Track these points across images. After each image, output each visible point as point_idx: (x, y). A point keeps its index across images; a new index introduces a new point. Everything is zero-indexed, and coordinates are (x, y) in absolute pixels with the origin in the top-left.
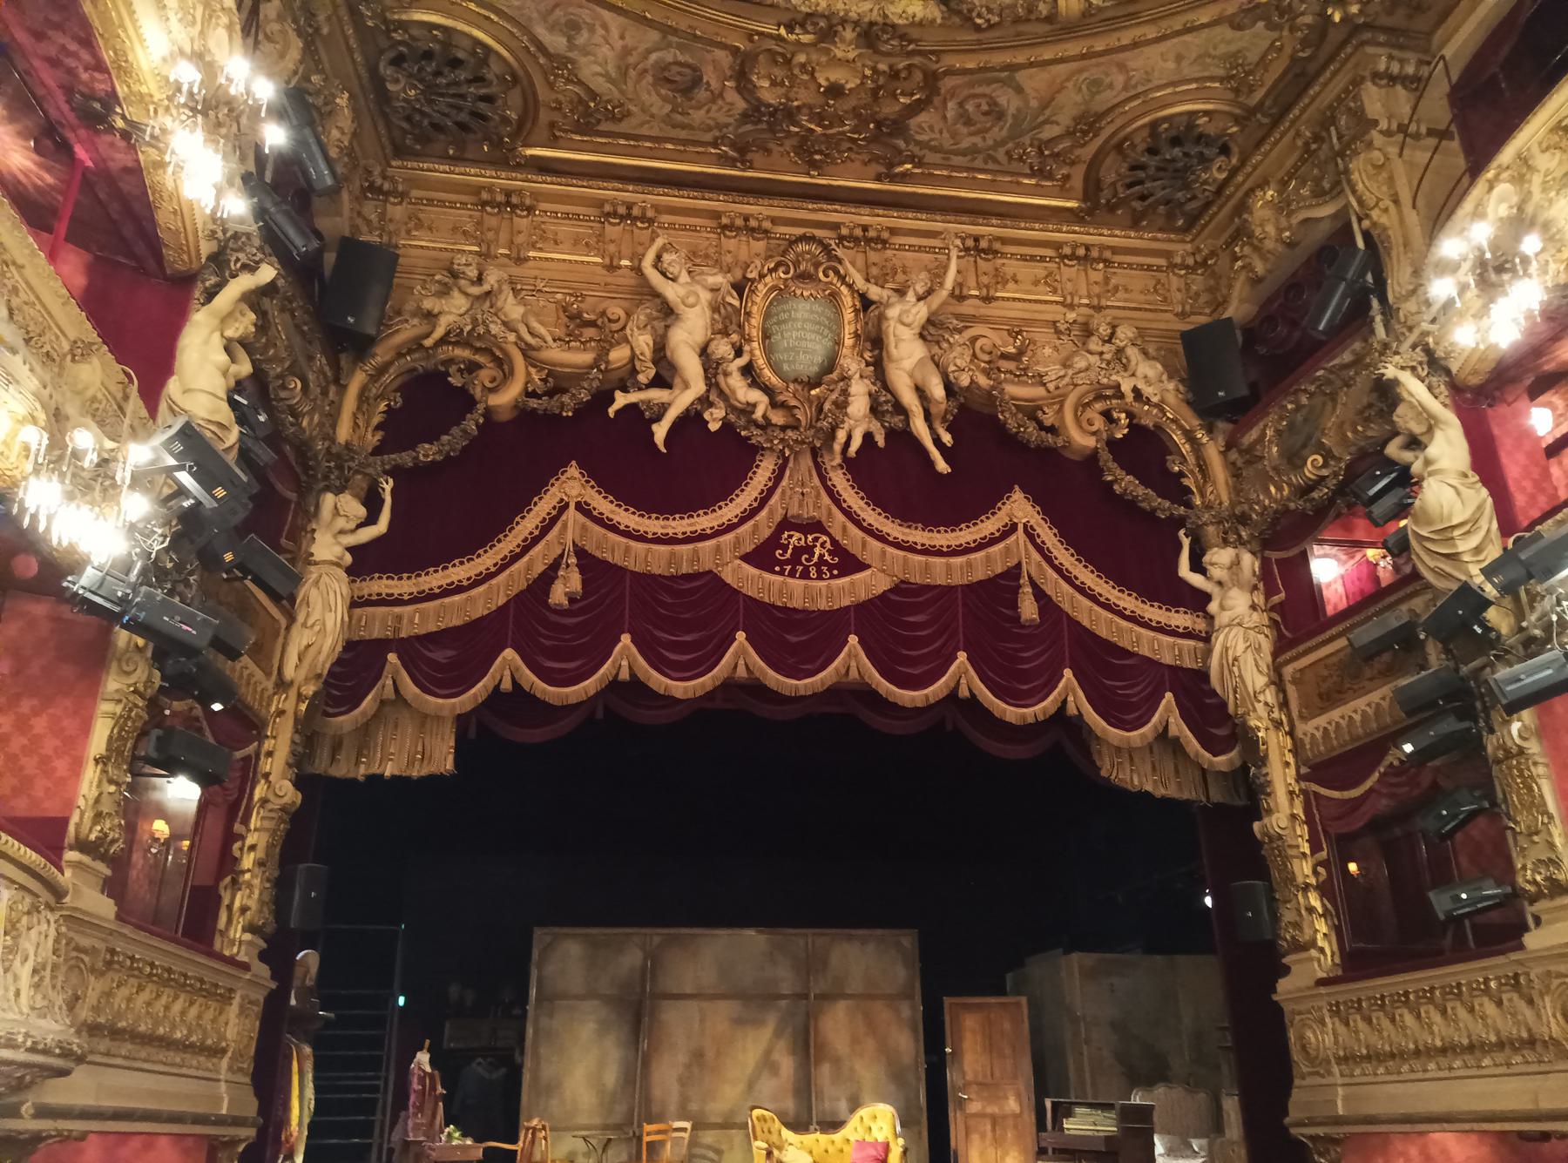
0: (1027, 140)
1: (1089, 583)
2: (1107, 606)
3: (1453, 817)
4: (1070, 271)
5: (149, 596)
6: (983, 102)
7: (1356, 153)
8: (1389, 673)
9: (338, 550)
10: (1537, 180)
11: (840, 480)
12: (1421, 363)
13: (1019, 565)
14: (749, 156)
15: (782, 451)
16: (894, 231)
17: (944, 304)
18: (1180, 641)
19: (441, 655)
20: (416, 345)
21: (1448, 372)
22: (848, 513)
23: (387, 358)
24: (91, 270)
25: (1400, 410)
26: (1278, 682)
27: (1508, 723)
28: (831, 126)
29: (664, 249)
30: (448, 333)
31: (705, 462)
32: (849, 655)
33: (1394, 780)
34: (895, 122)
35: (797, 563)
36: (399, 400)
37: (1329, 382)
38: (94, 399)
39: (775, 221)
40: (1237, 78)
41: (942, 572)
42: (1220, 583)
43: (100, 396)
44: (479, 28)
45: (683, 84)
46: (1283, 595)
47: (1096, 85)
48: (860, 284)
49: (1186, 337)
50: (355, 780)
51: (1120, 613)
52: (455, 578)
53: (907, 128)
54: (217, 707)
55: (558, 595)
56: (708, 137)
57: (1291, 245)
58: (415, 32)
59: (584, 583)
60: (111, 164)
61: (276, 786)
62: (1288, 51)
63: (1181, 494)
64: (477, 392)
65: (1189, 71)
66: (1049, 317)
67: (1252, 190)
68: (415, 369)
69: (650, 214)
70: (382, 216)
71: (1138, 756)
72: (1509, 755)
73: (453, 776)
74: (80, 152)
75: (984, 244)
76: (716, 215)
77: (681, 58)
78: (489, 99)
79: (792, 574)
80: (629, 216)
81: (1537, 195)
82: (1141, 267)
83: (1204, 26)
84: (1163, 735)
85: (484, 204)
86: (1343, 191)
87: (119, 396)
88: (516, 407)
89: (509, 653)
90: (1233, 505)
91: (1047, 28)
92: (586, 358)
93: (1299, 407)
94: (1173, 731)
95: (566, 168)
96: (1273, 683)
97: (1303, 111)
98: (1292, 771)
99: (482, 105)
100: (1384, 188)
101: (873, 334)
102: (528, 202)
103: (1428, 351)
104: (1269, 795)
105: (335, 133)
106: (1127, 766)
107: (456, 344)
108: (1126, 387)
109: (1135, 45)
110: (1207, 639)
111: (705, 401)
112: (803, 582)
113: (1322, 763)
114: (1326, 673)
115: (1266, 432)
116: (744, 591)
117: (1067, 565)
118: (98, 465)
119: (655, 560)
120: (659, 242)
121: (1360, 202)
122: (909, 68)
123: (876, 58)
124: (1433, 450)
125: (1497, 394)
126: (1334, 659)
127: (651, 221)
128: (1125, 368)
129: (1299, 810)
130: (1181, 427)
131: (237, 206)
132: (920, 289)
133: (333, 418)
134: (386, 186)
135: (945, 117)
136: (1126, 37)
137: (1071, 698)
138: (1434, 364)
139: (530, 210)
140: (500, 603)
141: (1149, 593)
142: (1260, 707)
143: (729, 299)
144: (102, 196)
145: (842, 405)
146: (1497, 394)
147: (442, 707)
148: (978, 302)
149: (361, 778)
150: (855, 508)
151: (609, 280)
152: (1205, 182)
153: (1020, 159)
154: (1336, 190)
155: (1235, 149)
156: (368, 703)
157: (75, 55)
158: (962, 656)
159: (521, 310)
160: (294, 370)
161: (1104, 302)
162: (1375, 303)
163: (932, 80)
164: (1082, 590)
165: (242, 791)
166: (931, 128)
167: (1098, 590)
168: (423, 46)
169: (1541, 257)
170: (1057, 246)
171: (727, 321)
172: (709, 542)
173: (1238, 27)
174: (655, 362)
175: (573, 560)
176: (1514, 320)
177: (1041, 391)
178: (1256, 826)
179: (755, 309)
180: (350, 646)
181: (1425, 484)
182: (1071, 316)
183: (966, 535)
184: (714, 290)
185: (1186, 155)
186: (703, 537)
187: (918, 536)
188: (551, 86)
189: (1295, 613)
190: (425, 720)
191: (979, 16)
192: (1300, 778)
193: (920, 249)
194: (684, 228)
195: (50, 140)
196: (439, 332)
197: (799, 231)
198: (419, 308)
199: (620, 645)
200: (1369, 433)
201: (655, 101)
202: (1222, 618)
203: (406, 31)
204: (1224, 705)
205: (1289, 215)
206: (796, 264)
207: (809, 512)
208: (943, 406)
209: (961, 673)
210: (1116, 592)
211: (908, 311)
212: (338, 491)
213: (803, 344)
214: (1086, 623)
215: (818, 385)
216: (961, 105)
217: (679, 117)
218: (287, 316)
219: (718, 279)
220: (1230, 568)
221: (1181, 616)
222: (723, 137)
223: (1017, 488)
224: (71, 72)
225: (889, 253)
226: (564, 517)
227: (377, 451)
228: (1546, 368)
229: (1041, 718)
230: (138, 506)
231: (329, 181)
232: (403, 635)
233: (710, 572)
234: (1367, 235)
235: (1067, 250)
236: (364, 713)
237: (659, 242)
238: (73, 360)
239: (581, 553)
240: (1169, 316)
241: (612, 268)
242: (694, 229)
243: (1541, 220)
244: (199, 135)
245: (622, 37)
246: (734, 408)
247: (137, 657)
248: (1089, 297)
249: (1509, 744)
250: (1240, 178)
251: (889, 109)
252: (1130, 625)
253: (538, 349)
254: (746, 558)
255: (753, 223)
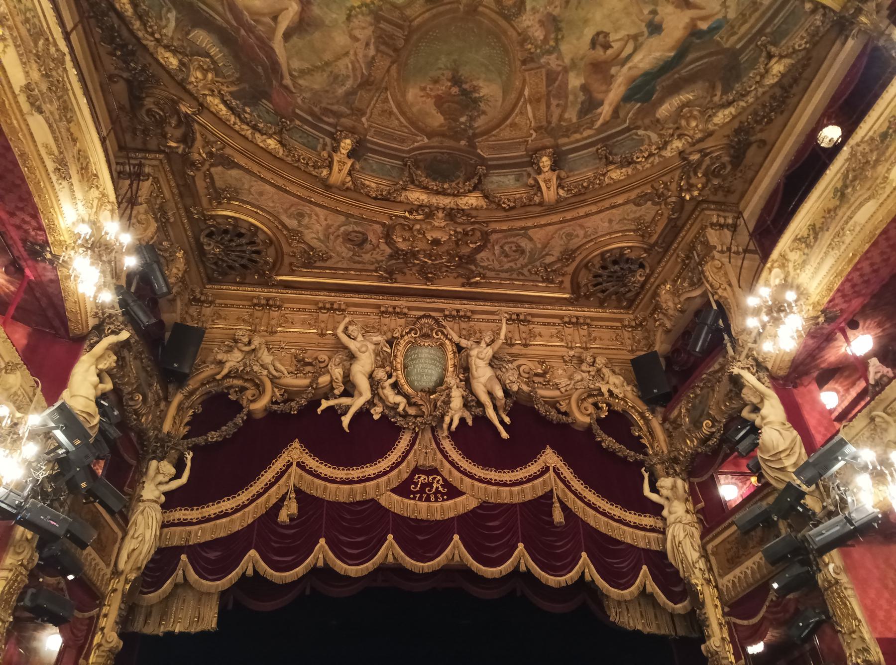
0: (538, 263)
1: (593, 500)
2: (604, 514)
3: (806, 626)
4: (569, 330)
5: (33, 504)
6: (513, 245)
7: (706, 262)
8: (762, 541)
9: (157, 493)
10: (791, 265)
11: (447, 445)
12: (752, 366)
13: (552, 490)
14: (394, 276)
15: (414, 429)
16: (473, 312)
17: (500, 348)
18: (648, 534)
19: (212, 555)
20: (212, 379)
21: (767, 369)
22: (452, 463)
23: (195, 386)
24: (30, 336)
25: (744, 391)
26: (705, 555)
27: (827, 565)
28: (436, 260)
29: (350, 323)
30: (230, 372)
31: (371, 437)
32: (454, 547)
33: (775, 609)
34: (469, 257)
35: (423, 493)
36: (201, 409)
37: (709, 381)
38: (15, 394)
39: (409, 308)
40: (642, 230)
41: (506, 496)
42: (667, 498)
43: (19, 393)
44: (253, 218)
45: (359, 242)
46: (703, 504)
47: (570, 236)
48: (456, 338)
49: (636, 363)
50: (157, 636)
51: (612, 518)
52: (224, 509)
53: (475, 260)
54: (71, 577)
55: (284, 516)
56: (372, 267)
57: (682, 311)
58: (219, 220)
59: (299, 509)
60: (43, 278)
61: (107, 636)
62: (666, 215)
63: (642, 449)
64: (244, 403)
65: (616, 227)
66: (560, 354)
67: (659, 286)
68: (211, 392)
69: (343, 307)
70: (199, 313)
71: (630, 606)
72: (831, 585)
73: (216, 632)
74: (27, 272)
75: (522, 317)
76: (378, 307)
77: (356, 229)
78: (258, 252)
79: (420, 499)
80: (332, 308)
81: (792, 273)
82: (607, 327)
83: (620, 205)
84: (643, 592)
85: (255, 305)
86: (703, 283)
87: (31, 394)
88: (265, 410)
89: (253, 552)
90: (669, 452)
91: (539, 209)
92: (306, 382)
93: (696, 396)
94: (649, 589)
95: (296, 285)
96: (702, 556)
97: (679, 244)
98: (719, 611)
99: (254, 255)
100: (723, 279)
101: (464, 364)
102: (278, 303)
103: (756, 360)
104: (708, 626)
105: (174, 270)
106: (626, 614)
107: (235, 377)
108: (604, 389)
109: (587, 215)
110: (663, 533)
111: (371, 403)
112: (426, 504)
113: (736, 603)
114: (729, 546)
115: (681, 410)
116: (392, 510)
117: (579, 490)
118: (11, 426)
119: (340, 494)
120: (347, 320)
121: (712, 286)
122: (473, 230)
123: (456, 225)
124: (764, 412)
125: (798, 381)
126: (733, 538)
127: (344, 310)
128: (603, 379)
129: (726, 635)
130: (637, 411)
131: (108, 297)
132: (488, 340)
133: (162, 419)
134: (203, 298)
135: (494, 254)
136: (582, 212)
137: (587, 570)
138: (759, 366)
139: (279, 307)
140: (250, 521)
141: (628, 506)
142: (697, 571)
143: (385, 349)
144: (38, 295)
145: (447, 403)
146: (798, 381)
147: (212, 586)
148: (522, 347)
149: (161, 634)
150: (456, 460)
151: (320, 341)
152: (634, 282)
153: (536, 273)
154: (700, 283)
155: (647, 265)
156: (167, 585)
157: (28, 223)
158: (521, 546)
159: (271, 358)
160: (138, 390)
161: (588, 346)
162: (726, 337)
163: (485, 236)
164: (589, 504)
165: (86, 639)
166: (488, 259)
167: (598, 504)
168: (223, 227)
169: (798, 303)
170: (561, 317)
171: (383, 360)
172: (373, 482)
173: (638, 205)
174: (344, 383)
175: (293, 495)
176: (792, 337)
177: (557, 393)
178: (703, 647)
179: (399, 353)
180: (160, 551)
181: (763, 430)
182: (572, 353)
183: (520, 474)
184: (377, 344)
185: (622, 269)
186: (369, 479)
187: (493, 475)
188: (290, 244)
189: (711, 514)
190: (202, 596)
191: (504, 203)
192: (724, 614)
193: (488, 321)
194: (361, 314)
195: (15, 269)
196: (225, 371)
197: (422, 313)
198: (215, 359)
199: (318, 545)
200: (733, 406)
201: (344, 251)
202: (671, 519)
203: (214, 220)
204: (678, 571)
205: (679, 296)
206: (421, 329)
207: (429, 463)
208: (503, 402)
209: (521, 557)
210: (608, 505)
211: (481, 352)
212: (160, 459)
213: (426, 371)
214: (592, 524)
215: (435, 393)
216: (502, 247)
217: (357, 258)
218: (138, 362)
219: (378, 338)
220: (672, 489)
221: (647, 518)
222: (380, 267)
223: (548, 446)
224: (26, 231)
225: (472, 323)
226: (289, 471)
227: (185, 437)
228: (823, 366)
229: (570, 583)
230: (31, 450)
231: (165, 290)
232: (191, 543)
233: (373, 499)
234: (717, 302)
235: (567, 319)
236: (164, 592)
237: (347, 320)
238: (6, 372)
239: (298, 491)
240: (625, 352)
241: (322, 335)
242: (366, 314)
243: (795, 284)
244: (88, 260)
245: (326, 220)
246: (388, 407)
247: (26, 544)
248: (581, 343)
249: (830, 578)
250: (652, 280)
251: (465, 251)
252: (618, 525)
253: (279, 378)
254: (394, 491)
255: (398, 310)
